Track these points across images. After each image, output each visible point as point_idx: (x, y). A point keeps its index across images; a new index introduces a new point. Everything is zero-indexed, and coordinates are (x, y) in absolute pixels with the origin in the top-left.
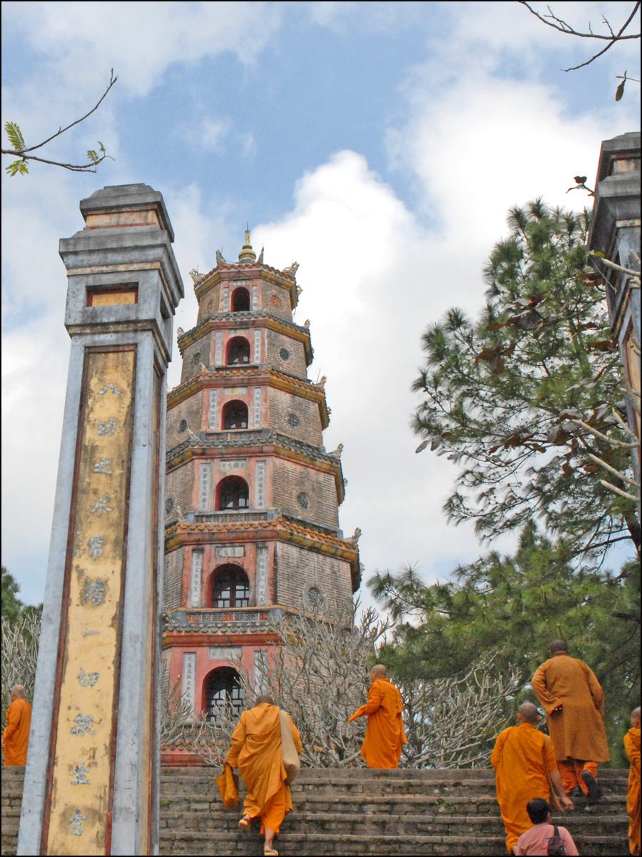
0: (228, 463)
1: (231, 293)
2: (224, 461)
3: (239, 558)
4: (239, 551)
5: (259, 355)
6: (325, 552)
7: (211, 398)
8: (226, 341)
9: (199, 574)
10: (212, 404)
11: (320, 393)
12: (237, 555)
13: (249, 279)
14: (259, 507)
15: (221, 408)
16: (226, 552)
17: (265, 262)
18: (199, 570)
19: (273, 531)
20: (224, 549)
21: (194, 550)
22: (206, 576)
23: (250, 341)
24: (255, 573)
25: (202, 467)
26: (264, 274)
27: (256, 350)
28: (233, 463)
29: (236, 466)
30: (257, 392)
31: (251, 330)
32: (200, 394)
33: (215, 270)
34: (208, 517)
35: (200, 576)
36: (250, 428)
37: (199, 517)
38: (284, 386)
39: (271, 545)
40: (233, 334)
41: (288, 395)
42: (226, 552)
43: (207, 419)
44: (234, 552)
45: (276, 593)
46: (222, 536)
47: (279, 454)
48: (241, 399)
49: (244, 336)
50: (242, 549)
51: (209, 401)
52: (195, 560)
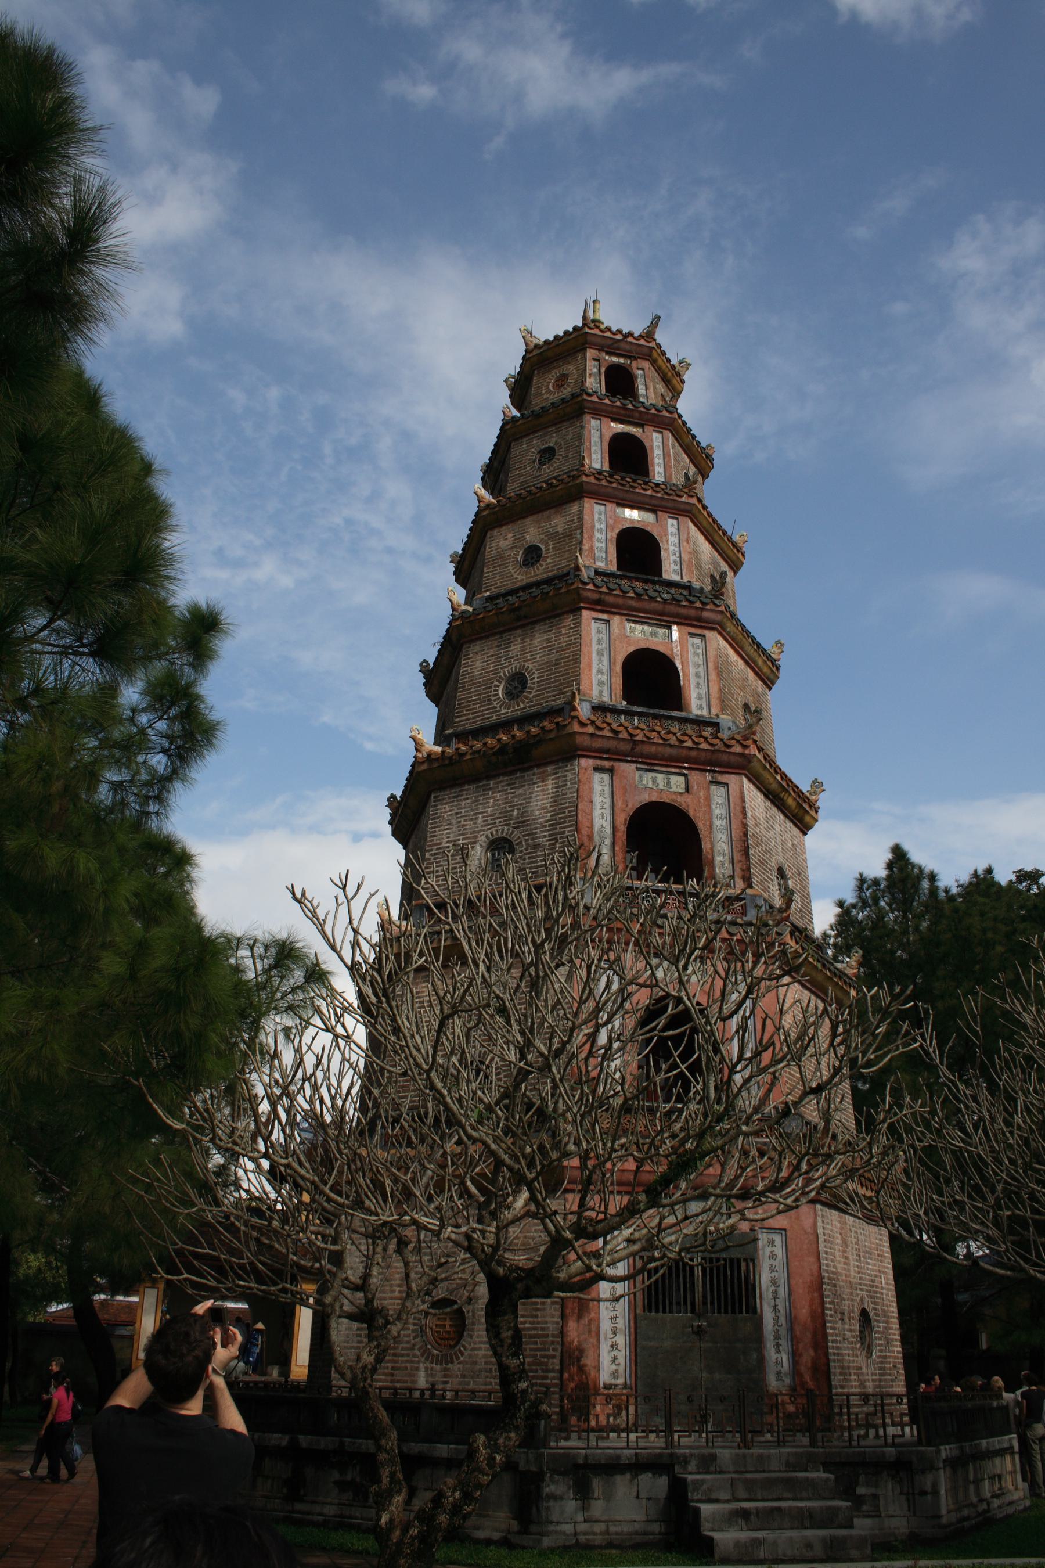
0: (639, 627)
1: (603, 370)
2: (634, 622)
3: (681, 794)
4: (677, 783)
5: (662, 470)
6: (788, 808)
7: (596, 516)
8: (608, 436)
9: (607, 812)
10: (597, 526)
11: (740, 555)
12: (674, 789)
13: (629, 357)
14: (699, 713)
15: (615, 536)
16: (654, 780)
17: (660, 337)
18: (607, 806)
19: (743, 755)
20: (651, 775)
21: (597, 769)
22: (622, 819)
23: (647, 445)
24: (711, 826)
25: (595, 625)
26: (655, 355)
27: (656, 461)
28: (648, 629)
29: (654, 634)
30: (671, 524)
31: (649, 429)
32: (575, 508)
33: (575, 328)
34: (615, 711)
35: (609, 818)
36: (665, 576)
37: (599, 708)
38: (708, 527)
39: (732, 780)
40: (619, 427)
41: (707, 543)
42: (654, 780)
43: (592, 548)
44: (669, 783)
45: (749, 869)
46: (653, 749)
47: (724, 630)
48: (648, 529)
49: (639, 435)
50: (682, 779)
51: (593, 520)
52: (597, 787)
